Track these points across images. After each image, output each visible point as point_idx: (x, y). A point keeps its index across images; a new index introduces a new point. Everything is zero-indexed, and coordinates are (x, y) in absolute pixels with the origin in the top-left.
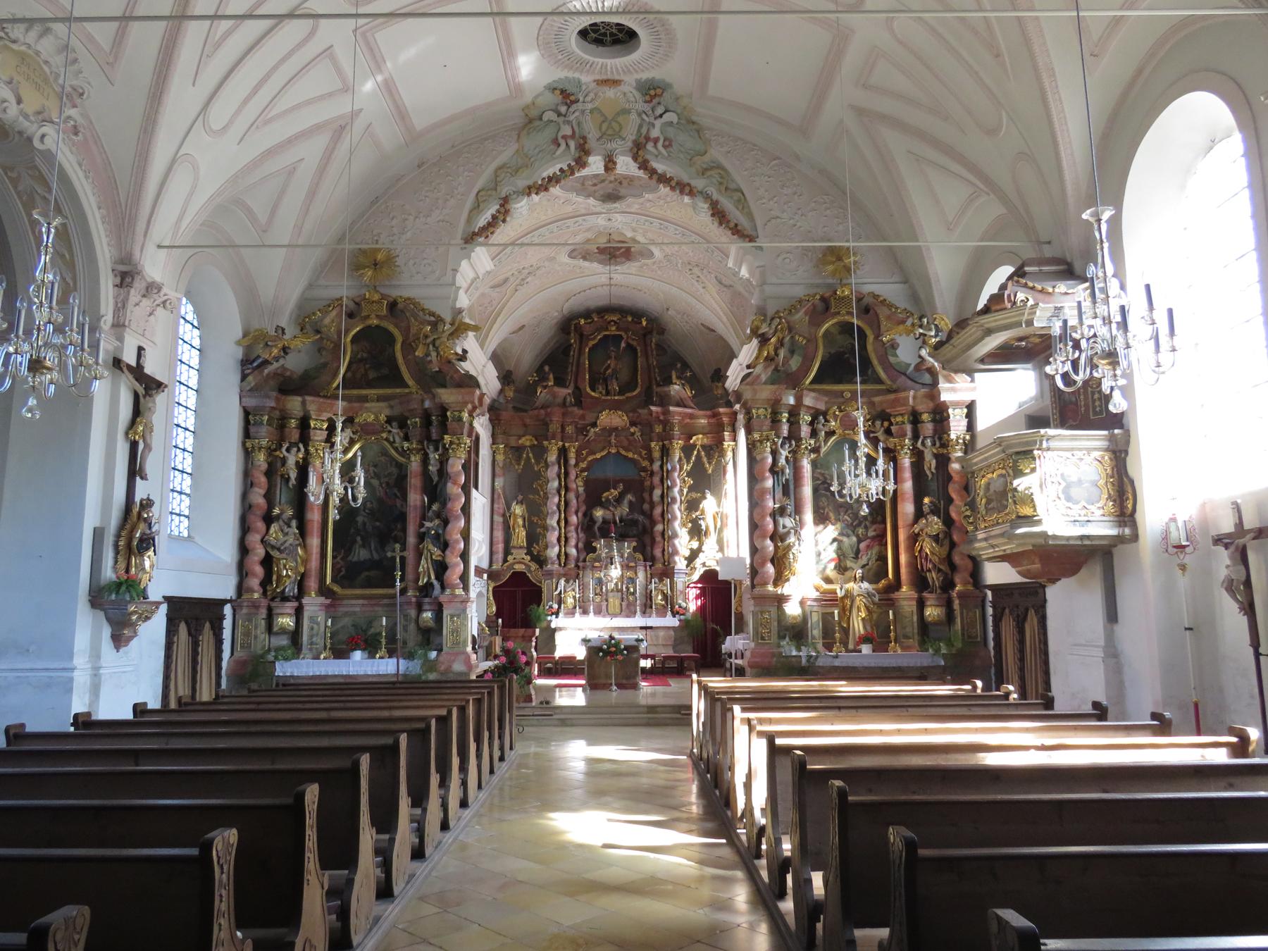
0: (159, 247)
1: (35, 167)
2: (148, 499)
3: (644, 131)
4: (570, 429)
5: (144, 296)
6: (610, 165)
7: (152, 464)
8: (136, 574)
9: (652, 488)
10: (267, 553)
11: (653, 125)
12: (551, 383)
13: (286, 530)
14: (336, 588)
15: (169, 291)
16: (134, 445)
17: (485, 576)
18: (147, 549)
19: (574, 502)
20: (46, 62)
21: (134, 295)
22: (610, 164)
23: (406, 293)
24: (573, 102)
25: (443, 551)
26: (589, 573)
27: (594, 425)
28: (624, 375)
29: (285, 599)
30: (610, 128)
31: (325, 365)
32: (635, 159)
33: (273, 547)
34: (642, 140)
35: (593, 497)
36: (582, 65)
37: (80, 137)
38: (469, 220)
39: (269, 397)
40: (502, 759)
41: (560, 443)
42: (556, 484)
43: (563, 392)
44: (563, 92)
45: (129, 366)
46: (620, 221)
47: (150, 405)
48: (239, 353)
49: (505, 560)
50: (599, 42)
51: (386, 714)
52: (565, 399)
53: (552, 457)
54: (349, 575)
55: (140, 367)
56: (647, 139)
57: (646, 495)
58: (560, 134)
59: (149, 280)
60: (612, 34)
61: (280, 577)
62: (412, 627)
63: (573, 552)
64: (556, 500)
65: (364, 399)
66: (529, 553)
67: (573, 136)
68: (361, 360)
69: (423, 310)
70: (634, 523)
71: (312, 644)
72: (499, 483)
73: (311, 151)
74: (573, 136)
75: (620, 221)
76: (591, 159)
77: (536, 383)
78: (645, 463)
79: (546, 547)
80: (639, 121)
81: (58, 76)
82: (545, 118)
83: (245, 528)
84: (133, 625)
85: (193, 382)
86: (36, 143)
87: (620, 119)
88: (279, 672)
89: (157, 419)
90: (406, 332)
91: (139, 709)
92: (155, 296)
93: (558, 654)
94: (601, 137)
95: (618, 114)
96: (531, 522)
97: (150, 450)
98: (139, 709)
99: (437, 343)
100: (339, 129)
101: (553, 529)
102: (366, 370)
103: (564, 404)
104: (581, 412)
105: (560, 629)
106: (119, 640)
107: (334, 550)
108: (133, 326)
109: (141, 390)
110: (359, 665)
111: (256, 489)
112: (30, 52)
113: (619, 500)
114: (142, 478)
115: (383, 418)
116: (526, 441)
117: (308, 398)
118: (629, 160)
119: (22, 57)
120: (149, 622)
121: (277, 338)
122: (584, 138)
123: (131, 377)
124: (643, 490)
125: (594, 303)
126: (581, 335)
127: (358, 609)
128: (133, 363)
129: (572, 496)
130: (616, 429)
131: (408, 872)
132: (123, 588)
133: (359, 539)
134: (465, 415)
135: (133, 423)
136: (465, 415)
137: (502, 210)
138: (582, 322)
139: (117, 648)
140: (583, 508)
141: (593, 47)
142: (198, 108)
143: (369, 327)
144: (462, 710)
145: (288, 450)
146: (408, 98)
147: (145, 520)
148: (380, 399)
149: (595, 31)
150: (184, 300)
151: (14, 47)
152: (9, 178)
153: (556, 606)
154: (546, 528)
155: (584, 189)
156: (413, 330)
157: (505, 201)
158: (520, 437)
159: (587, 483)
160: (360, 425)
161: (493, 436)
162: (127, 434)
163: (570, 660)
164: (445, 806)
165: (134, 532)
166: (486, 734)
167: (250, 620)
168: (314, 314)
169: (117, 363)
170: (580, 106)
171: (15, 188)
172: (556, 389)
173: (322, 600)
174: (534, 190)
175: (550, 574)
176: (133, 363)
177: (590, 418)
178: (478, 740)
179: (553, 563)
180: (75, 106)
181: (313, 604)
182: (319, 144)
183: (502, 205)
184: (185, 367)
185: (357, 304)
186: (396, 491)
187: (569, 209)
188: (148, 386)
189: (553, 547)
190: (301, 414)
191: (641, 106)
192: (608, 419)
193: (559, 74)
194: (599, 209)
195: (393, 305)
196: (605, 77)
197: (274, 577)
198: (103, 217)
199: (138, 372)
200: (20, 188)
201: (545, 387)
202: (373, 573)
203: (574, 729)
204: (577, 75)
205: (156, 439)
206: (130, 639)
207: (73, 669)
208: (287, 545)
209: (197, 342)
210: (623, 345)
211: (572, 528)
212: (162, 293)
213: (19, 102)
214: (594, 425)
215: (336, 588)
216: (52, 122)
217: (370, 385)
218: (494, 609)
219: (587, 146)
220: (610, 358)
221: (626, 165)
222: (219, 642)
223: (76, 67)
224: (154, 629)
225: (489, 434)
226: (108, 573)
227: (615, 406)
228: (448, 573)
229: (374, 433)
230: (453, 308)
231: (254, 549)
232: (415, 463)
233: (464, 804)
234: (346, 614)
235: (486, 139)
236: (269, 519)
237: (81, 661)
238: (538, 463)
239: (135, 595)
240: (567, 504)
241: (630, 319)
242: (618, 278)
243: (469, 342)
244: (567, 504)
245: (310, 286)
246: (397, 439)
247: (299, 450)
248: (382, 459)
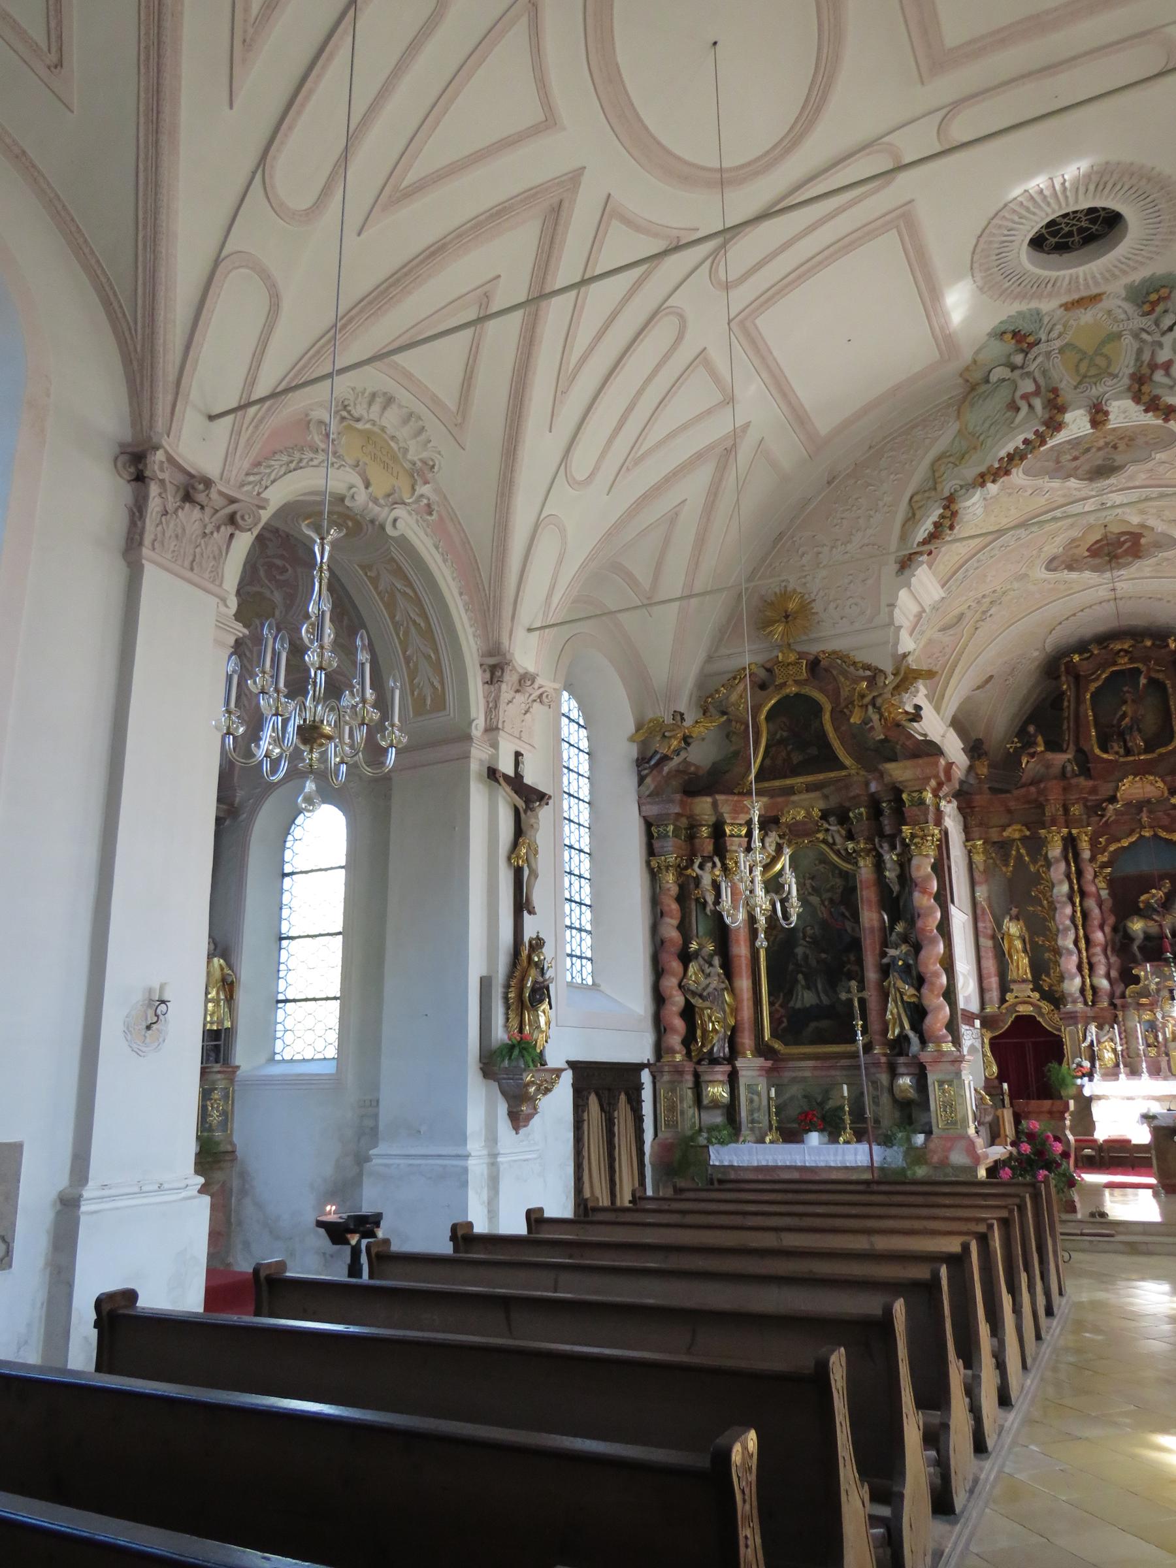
0: (530, 630)
1: (393, 559)
2: (538, 938)
3: (1146, 357)
4: (1076, 810)
5: (517, 691)
6: (1100, 417)
7: (539, 895)
8: (531, 1034)
10: (687, 1001)
11: (1160, 345)
12: (1040, 749)
13: (708, 971)
14: (777, 1045)
15: (545, 682)
16: (518, 872)
17: (977, 1023)
18: (541, 1001)
19: (1096, 912)
20: (393, 438)
21: (506, 690)
22: (1098, 415)
23: (829, 647)
24: (1031, 345)
25: (918, 989)
26: (1133, 1014)
27: (1113, 799)
28: (1151, 722)
29: (714, 1061)
30: (1092, 365)
31: (736, 754)
32: (1137, 399)
33: (694, 994)
34: (1145, 370)
35: (1125, 901)
36: (1040, 288)
37: (435, 516)
38: (904, 537)
39: (672, 801)
40: (1049, 1312)
41: (1065, 831)
42: (1065, 888)
43: (1060, 759)
44: (1016, 334)
45: (506, 777)
46: (1121, 502)
47: (533, 821)
48: (633, 751)
49: (1003, 1000)
50: (1062, 248)
51: (859, 1243)
52: (1064, 767)
53: (1055, 850)
54: (794, 1026)
55: (518, 776)
56: (1153, 367)
58: (1019, 394)
59: (522, 671)
60: (1081, 230)
61: (705, 1031)
62: (885, 1099)
63: (1104, 984)
64: (1068, 910)
65: (790, 791)
66: (1037, 988)
67: (1037, 393)
68: (782, 742)
69: (854, 664)
71: (753, 1121)
72: (981, 893)
73: (694, 487)
74: (1037, 393)
75: (1121, 502)
76: (1068, 417)
77: (1018, 753)
79: (1062, 978)
80: (1136, 345)
81: (406, 450)
82: (994, 378)
83: (658, 971)
84: (532, 1100)
85: (585, 793)
86: (389, 530)
87: (1105, 350)
88: (714, 1160)
89: (542, 836)
90: (835, 696)
91: (535, 1218)
92: (529, 689)
93: (1101, 1134)
94: (1080, 383)
95: (1103, 343)
96: (1032, 942)
97: (536, 877)
98: (535, 1218)
99: (879, 701)
100: (727, 451)
101: (1070, 953)
102: (788, 754)
103: (1063, 775)
104: (1090, 783)
105: (1099, 1098)
106: (518, 1120)
107: (770, 994)
108: (508, 727)
109: (521, 804)
110: (816, 1152)
111: (667, 920)
112: (376, 429)
114: (530, 913)
115: (816, 813)
116: (1014, 832)
117: (720, 797)
118: (1128, 403)
119: (368, 436)
120: (550, 1095)
121: (676, 727)
122: (1055, 391)
123: (508, 789)
125: (1088, 631)
126: (1077, 678)
127: (808, 1074)
128: (511, 773)
129: (1091, 903)
130: (1149, 801)
131: (930, 1546)
132: (516, 1052)
133: (800, 977)
134: (928, 796)
135: (515, 845)
136: (928, 796)
137: (948, 514)
138: (1076, 658)
139: (516, 1128)
140: (1111, 920)
141: (1055, 257)
142: (558, 460)
143: (787, 697)
144: (983, 1239)
145: (701, 867)
146: (806, 394)
147: (537, 964)
148: (810, 788)
149: (1054, 234)
150: (565, 695)
151: (359, 426)
152: (369, 578)
153: (1087, 1064)
154: (1057, 952)
155: (1059, 470)
156: (845, 692)
157: (950, 502)
158: (1004, 828)
159: (1111, 883)
160: (788, 826)
161: (966, 829)
162: (509, 859)
163: (1121, 1145)
164: (975, 1410)
165: (525, 981)
166: (1024, 1277)
167: (673, 1090)
168: (717, 691)
169: (492, 774)
170: (1043, 347)
171: (376, 588)
172: (1050, 756)
173: (760, 1061)
174: (990, 478)
175: (1072, 1018)
176: (511, 773)
177: (1105, 790)
178: (1013, 1290)
179: (1074, 1002)
180: (426, 482)
181: (750, 1067)
182: (703, 476)
183: (946, 507)
184: (573, 776)
185: (769, 671)
186: (843, 909)
187: (1041, 501)
188: (529, 798)
189: (1072, 978)
190: (713, 819)
191: (1139, 322)
192: (1132, 788)
193: (1006, 311)
194: (1083, 494)
195: (814, 664)
196: (1076, 297)
197: (699, 1033)
198: (466, 604)
199: (516, 782)
200: (380, 588)
201: (1032, 755)
202: (824, 1024)
203: (1153, 1260)
204: (1034, 304)
205: (543, 863)
206: (529, 1117)
207: (467, 1157)
208: (710, 989)
209: (584, 745)
210: (1143, 681)
211: (1098, 950)
212: (536, 686)
213: (367, 485)
214: (1113, 799)
215: (777, 1045)
216: (404, 503)
217: (795, 772)
218: (995, 1069)
219: (1060, 401)
220: (1125, 702)
221: (1125, 413)
222: (639, 1119)
223: (423, 437)
224: (558, 1103)
225: (960, 828)
226: (500, 1034)
227: (1141, 770)
228: (928, 1020)
229: (807, 834)
230: (894, 655)
231: (671, 996)
232: (865, 869)
233: (1004, 1400)
234: (794, 1080)
235: (913, 427)
236: (686, 958)
237: (475, 1146)
238: (1034, 861)
239: (529, 1059)
240: (1085, 915)
241: (1149, 643)
242: (1124, 587)
243: (920, 695)
244: (1085, 915)
245: (710, 659)
246: (838, 840)
247: (714, 865)
248: (821, 867)
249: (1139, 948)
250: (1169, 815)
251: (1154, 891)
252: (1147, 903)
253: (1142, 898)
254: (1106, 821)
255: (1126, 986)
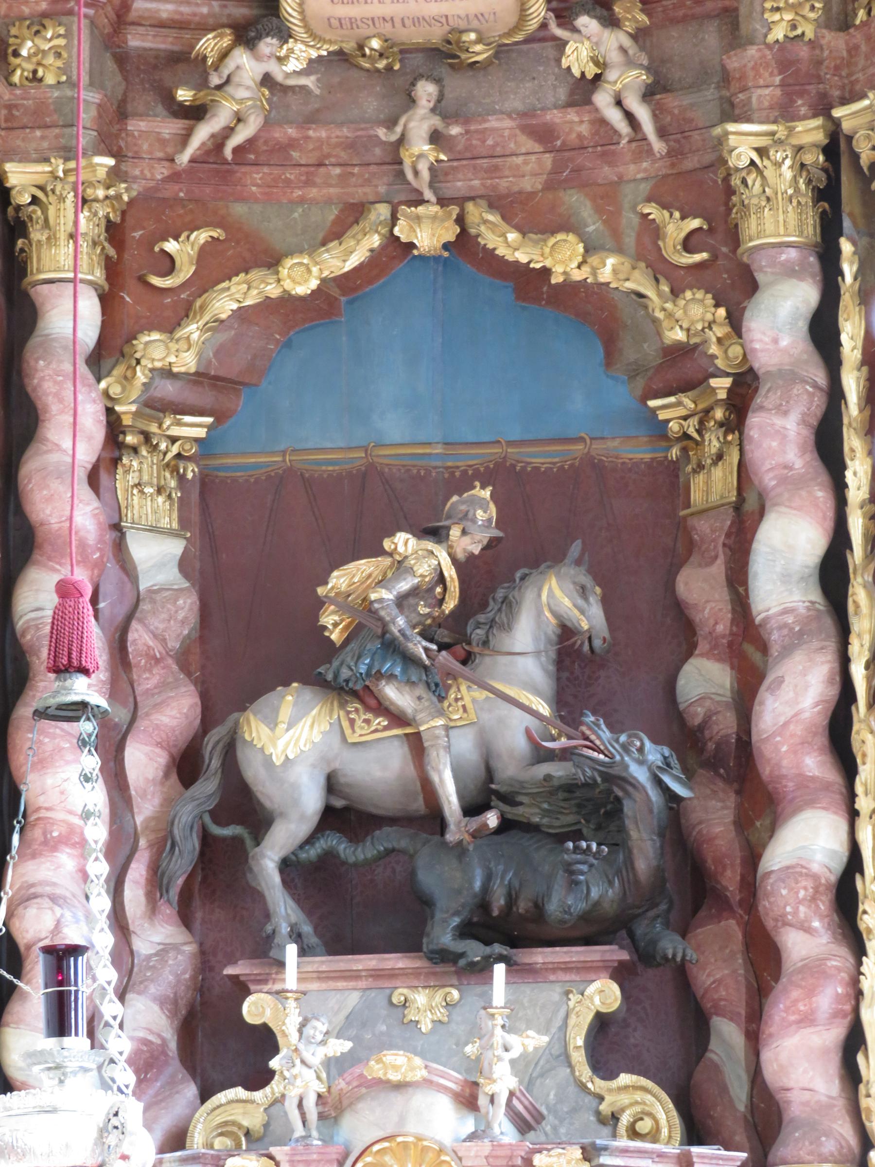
9: (745, 518)
57: (701, 588)
70: (598, 804)
78: (688, 317)
113: (463, 631)
124: (681, 549)
130: (443, 56)
140: (175, 711)
159: (210, 504)
249: (286, 865)
250: (544, 135)
251: (403, 542)
252: (367, 622)
253: (340, 580)
254: (219, 141)
255: (205, 1095)
